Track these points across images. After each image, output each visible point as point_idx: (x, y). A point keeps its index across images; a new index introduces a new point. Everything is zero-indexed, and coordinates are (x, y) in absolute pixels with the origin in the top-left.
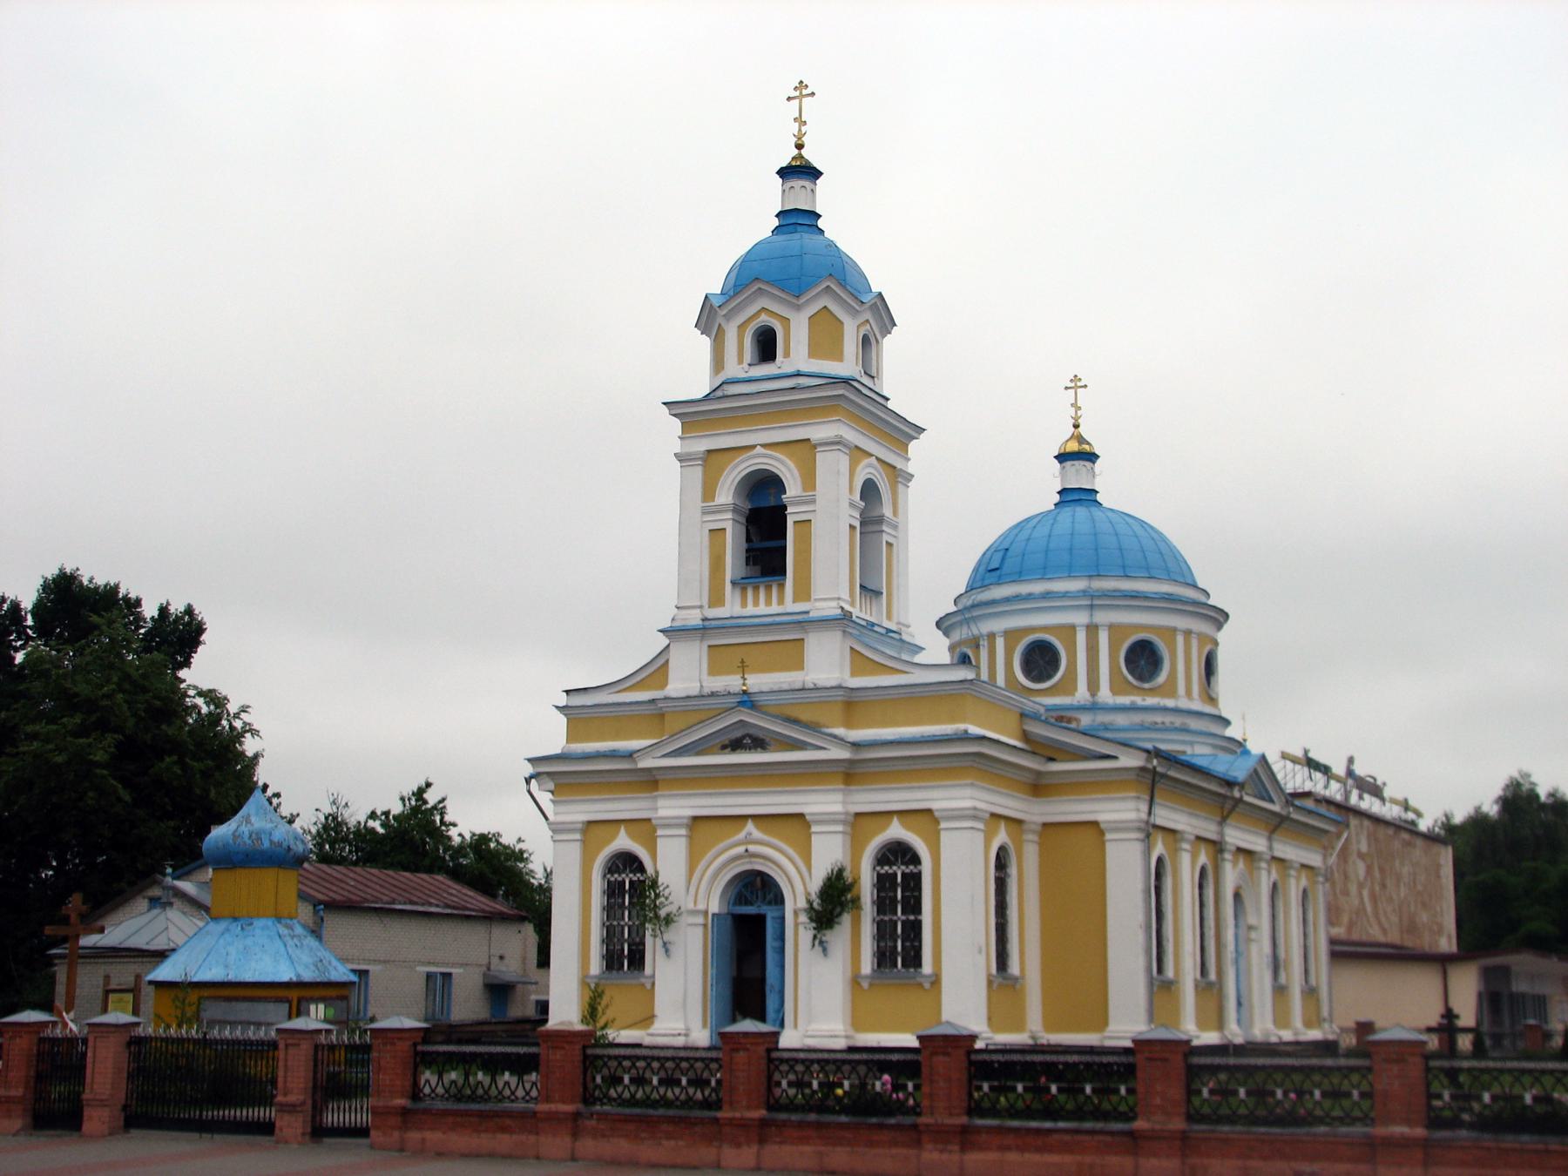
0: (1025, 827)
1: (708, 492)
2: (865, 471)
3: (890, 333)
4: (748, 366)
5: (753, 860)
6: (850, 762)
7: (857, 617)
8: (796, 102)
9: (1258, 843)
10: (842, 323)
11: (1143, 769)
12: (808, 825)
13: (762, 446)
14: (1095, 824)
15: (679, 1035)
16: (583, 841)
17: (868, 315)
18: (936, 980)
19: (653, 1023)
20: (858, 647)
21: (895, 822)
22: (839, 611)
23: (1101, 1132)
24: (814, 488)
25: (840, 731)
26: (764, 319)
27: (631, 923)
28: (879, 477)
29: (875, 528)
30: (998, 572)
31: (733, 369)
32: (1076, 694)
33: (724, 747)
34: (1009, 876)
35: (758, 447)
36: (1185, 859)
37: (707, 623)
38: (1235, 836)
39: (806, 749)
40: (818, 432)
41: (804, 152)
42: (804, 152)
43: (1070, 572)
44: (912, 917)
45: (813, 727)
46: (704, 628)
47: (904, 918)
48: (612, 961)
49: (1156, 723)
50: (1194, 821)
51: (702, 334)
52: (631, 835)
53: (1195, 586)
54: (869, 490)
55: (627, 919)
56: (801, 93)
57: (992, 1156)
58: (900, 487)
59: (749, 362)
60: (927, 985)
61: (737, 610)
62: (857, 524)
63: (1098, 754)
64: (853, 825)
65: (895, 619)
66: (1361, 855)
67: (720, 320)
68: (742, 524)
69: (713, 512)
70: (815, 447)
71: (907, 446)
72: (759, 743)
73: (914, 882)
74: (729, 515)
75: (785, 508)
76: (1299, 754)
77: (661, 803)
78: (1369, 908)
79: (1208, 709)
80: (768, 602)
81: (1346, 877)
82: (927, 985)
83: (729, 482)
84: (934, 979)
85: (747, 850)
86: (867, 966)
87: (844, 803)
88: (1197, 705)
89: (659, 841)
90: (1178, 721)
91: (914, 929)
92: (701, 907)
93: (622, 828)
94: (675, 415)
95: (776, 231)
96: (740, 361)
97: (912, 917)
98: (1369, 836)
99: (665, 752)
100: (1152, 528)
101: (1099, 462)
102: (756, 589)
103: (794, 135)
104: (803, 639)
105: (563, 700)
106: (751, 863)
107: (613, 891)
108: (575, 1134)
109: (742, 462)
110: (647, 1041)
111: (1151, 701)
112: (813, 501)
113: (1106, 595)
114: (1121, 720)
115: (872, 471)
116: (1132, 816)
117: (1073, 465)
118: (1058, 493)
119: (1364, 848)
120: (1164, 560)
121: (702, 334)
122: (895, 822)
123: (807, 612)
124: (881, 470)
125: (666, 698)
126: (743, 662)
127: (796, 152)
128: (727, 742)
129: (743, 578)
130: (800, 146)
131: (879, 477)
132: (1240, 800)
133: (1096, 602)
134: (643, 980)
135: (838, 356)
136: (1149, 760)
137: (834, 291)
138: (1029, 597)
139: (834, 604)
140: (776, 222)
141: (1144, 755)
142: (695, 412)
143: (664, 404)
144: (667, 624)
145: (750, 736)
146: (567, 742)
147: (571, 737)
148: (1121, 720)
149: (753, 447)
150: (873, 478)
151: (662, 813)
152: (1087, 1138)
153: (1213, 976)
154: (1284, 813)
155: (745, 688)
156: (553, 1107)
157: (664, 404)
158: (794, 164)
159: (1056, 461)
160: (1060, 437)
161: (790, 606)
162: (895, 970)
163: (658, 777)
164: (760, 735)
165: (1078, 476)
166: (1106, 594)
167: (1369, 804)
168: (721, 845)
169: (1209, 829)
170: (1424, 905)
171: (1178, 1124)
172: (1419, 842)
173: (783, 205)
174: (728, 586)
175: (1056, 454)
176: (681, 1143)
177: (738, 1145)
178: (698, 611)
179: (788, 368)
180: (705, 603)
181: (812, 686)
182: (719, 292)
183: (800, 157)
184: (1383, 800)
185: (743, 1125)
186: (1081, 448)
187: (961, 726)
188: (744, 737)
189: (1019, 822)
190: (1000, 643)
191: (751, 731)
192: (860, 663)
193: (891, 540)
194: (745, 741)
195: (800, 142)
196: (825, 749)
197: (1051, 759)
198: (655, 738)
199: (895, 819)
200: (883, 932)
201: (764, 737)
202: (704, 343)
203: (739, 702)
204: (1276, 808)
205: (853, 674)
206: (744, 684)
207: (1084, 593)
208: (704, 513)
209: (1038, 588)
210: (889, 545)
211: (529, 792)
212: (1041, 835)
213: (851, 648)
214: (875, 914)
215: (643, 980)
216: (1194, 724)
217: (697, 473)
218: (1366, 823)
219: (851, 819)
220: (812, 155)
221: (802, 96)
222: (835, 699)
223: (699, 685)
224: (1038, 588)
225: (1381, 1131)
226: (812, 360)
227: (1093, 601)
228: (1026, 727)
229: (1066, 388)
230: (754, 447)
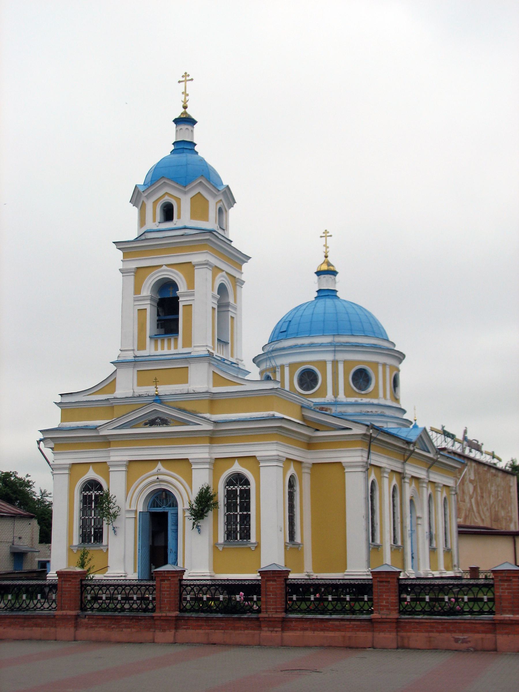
0: (303, 465)
1: (137, 290)
2: (221, 279)
3: (233, 207)
4: (158, 224)
5: (161, 483)
6: (213, 431)
7: (216, 355)
8: (183, 83)
9: (422, 474)
10: (207, 201)
11: (365, 435)
12: (190, 465)
13: (166, 265)
14: (340, 463)
17: (221, 197)
18: (258, 546)
20: (215, 371)
21: (236, 462)
22: (207, 353)
23: (354, 620)
24: (193, 288)
25: (207, 415)
26: (167, 199)
27: (95, 517)
28: (227, 282)
29: (224, 309)
30: (285, 333)
31: (150, 225)
32: (327, 397)
33: (146, 424)
34: (295, 491)
35: (164, 266)
36: (386, 481)
37: (136, 359)
38: (411, 470)
39: (189, 425)
40: (196, 258)
41: (187, 110)
42: (187, 110)
43: (323, 333)
44: (245, 513)
45: (193, 413)
46: (135, 361)
47: (241, 513)
48: (85, 538)
49: (368, 412)
50: (390, 462)
51: (133, 206)
53: (387, 340)
54: (222, 289)
55: (93, 516)
56: (186, 79)
57: (299, 633)
58: (238, 287)
59: (159, 221)
60: (253, 549)
61: (153, 352)
62: (216, 307)
63: (343, 427)
64: (214, 465)
65: (235, 357)
66: (471, 481)
67: (143, 199)
68: (156, 307)
69: (141, 300)
70: (194, 266)
71: (241, 266)
72: (164, 422)
73: (246, 494)
74: (148, 302)
75: (178, 298)
76: (439, 428)
77: (112, 454)
78: (475, 509)
79: (395, 404)
80: (169, 348)
81: (463, 492)
82: (253, 549)
84: (256, 545)
85: (158, 478)
86: (221, 538)
87: (209, 453)
88: (389, 403)
89: (111, 473)
90: (379, 410)
91: (246, 519)
92: (133, 508)
94: (118, 248)
95: (173, 152)
96: (154, 221)
97: (245, 513)
98: (475, 470)
100: (365, 310)
101: (338, 275)
102: (163, 340)
103: (182, 101)
105: (59, 399)
106: (160, 485)
107: (86, 500)
108: (76, 626)
111: (365, 400)
113: (342, 345)
114: (350, 410)
115: (224, 279)
116: (359, 459)
117: (324, 277)
118: (317, 291)
119: (472, 478)
120: (372, 328)
121: (133, 206)
123: (190, 353)
124: (229, 280)
125: (115, 398)
126: (156, 379)
127: (183, 110)
128: (147, 421)
129: (156, 335)
130: (185, 107)
131: (227, 282)
132: (413, 452)
133: (337, 349)
135: (205, 217)
136: (368, 430)
137: (205, 186)
138: (302, 346)
139: (204, 349)
140: (172, 147)
141: (366, 428)
142: (192, 241)
143: (114, 243)
144: (115, 359)
145: (160, 418)
146: (62, 421)
147: (64, 419)
148: (350, 410)
149: (161, 266)
150: (225, 283)
151: (112, 459)
152: (348, 623)
153: (399, 543)
154: (435, 458)
155: (157, 393)
156: (64, 612)
157: (114, 243)
158: (182, 116)
159: (315, 275)
160: (318, 263)
161: (181, 350)
164: (165, 417)
165: (327, 283)
166: (342, 345)
167: (474, 454)
169: (397, 466)
170: (502, 507)
171: (394, 615)
172: (500, 474)
173: (176, 139)
174: (148, 339)
175: (316, 271)
176: (133, 630)
177: (164, 631)
178: (132, 352)
179: (180, 225)
180: (136, 348)
181: (192, 392)
182: (143, 184)
183: (185, 113)
184: (481, 452)
185: (166, 619)
186: (329, 268)
187: (272, 413)
188: (156, 419)
189: (301, 463)
190: (287, 370)
191: (160, 416)
192: (218, 380)
193: (233, 315)
195: (185, 105)
196: (199, 424)
197: (317, 430)
198: (110, 420)
199: (236, 460)
200: (230, 520)
201: (167, 419)
202: (135, 211)
203: (153, 400)
204: (431, 455)
205: (214, 386)
206: (156, 391)
207: (331, 344)
208: (135, 301)
209: (306, 341)
210: (232, 318)
211: (39, 448)
212: (311, 469)
213: (213, 371)
214: (226, 512)
215: (102, 548)
216: (388, 412)
217: (131, 279)
218: (474, 464)
219: (213, 461)
220: (192, 112)
221: (186, 81)
222: (206, 398)
223: (132, 391)
224: (306, 341)
225: (498, 617)
226: (192, 220)
227: (336, 348)
228: (303, 414)
229: (321, 237)
230: (161, 266)
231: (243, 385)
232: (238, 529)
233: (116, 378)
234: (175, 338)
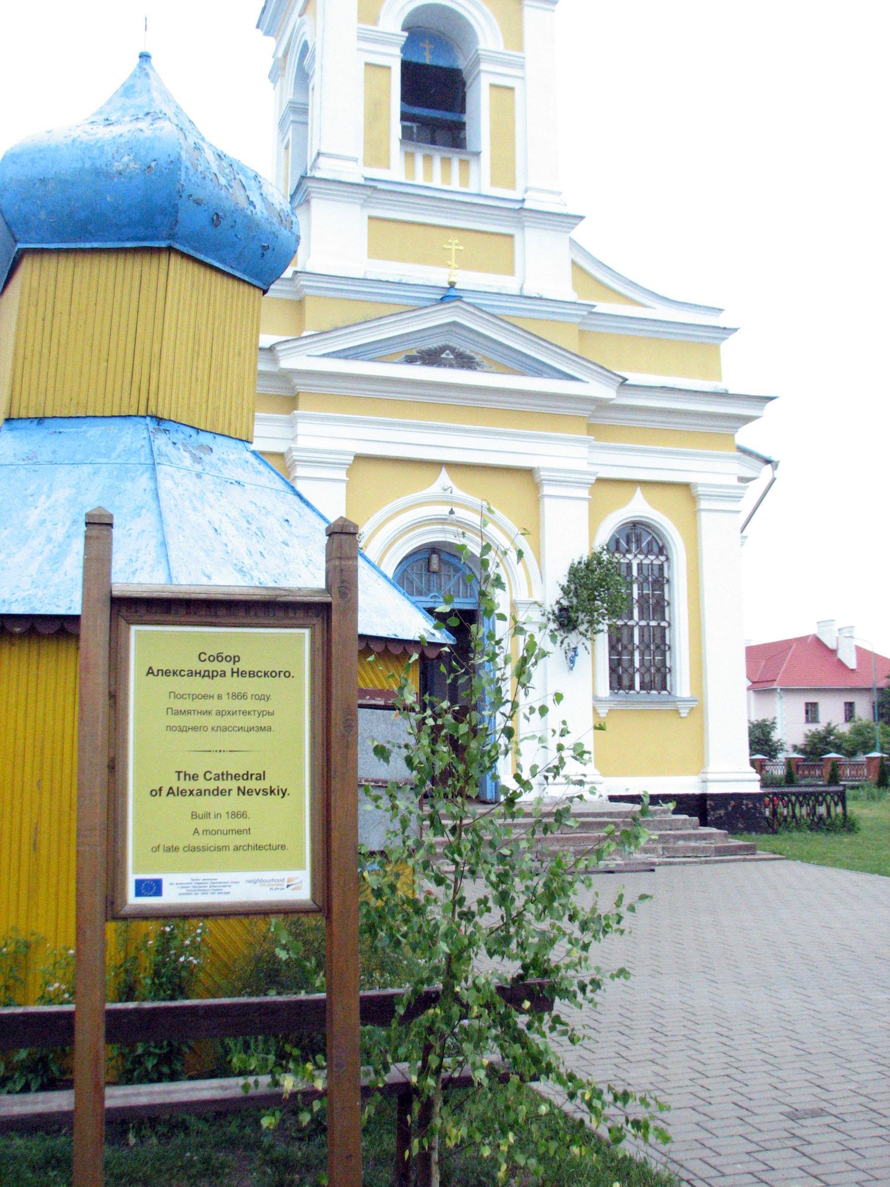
18: (698, 706)
69: (375, 41)
82: (684, 713)
85: (452, 512)
97: (653, 623)
106: (444, 531)
145: (453, 350)
151: (301, 443)
162: (632, 692)
163: (300, 389)
188: (443, 349)
198: (289, 335)
199: (639, 489)
201: (472, 354)
213: (574, 263)
231: (650, 307)
232: (637, 664)
234: (461, 161)
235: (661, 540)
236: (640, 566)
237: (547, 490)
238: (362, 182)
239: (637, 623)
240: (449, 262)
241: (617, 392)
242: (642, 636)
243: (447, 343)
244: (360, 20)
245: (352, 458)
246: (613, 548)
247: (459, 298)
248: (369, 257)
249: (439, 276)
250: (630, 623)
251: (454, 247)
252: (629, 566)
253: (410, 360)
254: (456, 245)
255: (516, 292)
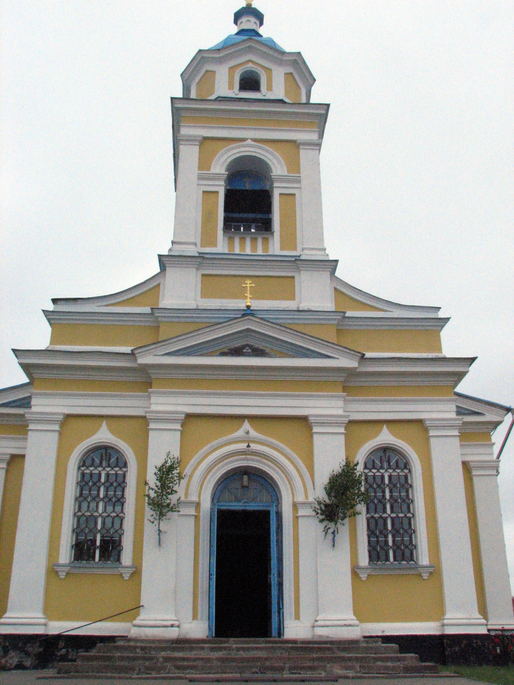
12: (310, 427)
13: (253, 140)
15: (172, 626)
16: (60, 433)
19: (138, 614)
20: (339, 287)
21: (385, 429)
26: (250, 66)
52: (113, 432)
69: (209, 179)
74: (223, 183)
82: (425, 576)
83: (225, 157)
85: (248, 446)
89: (151, 433)
93: (104, 422)
96: (231, 87)
99: (168, 351)
104: (293, 277)
105: (51, 307)
106: (248, 460)
109: (233, 148)
110: (134, 632)
112: (298, 181)
122: (385, 429)
134: (122, 570)
145: (251, 347)
146: (52, 342)
151: (154, 408)
162: (387, 563)
163: (153, 376)
168: (215, 443)
188: (244, 347)
194: (244, 351)
199: (385, 426)
213: (335, 289)
215: (122, 570)
232: (390, 543)
233: (159, 285)
234: (263, 239)
235: (404, 458)
236: (390, 477)
237: (315, 430)
238: (197, 255)
239: (389, 515)
240: (246, 295)
241: (359, 363)
242: (393, 525)
243: (247, 343)
244: (200, 168)
245: (184, 416)
246: (370, 466)
247: (253, 315)
248: (202, 298)
249: (241, 304)
250: (385, 515)
251: (248, 285)
252: (383, 477)
253: (223, 354)
254: (250, 284)
255: (296, 309)
